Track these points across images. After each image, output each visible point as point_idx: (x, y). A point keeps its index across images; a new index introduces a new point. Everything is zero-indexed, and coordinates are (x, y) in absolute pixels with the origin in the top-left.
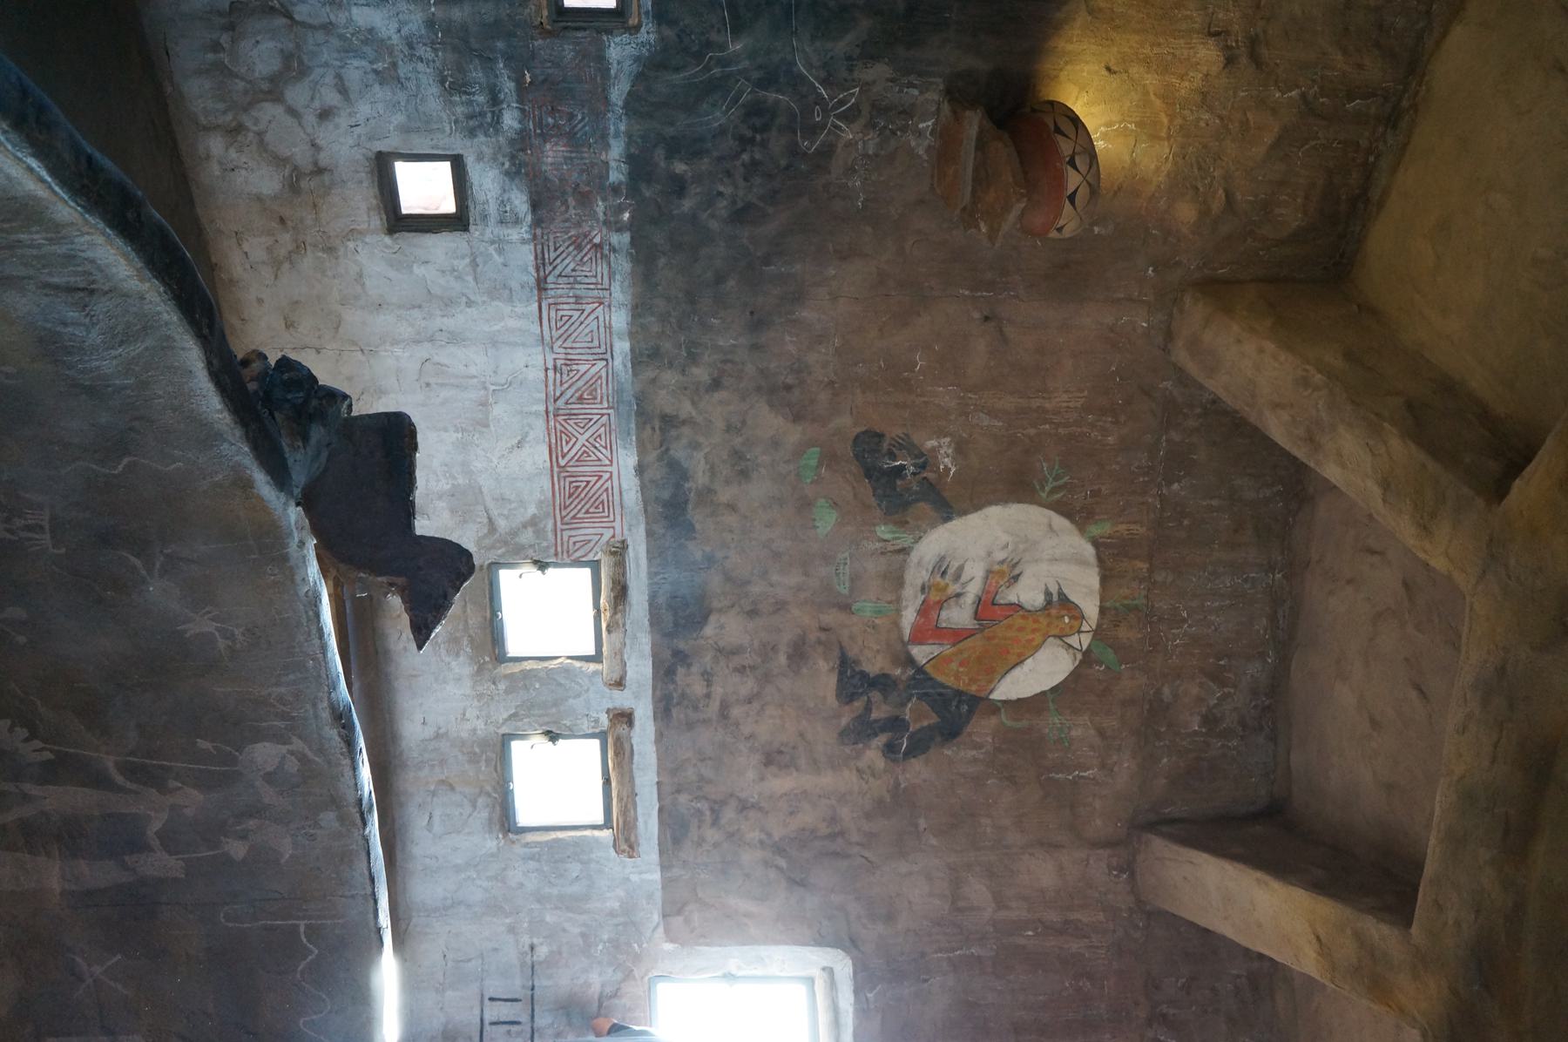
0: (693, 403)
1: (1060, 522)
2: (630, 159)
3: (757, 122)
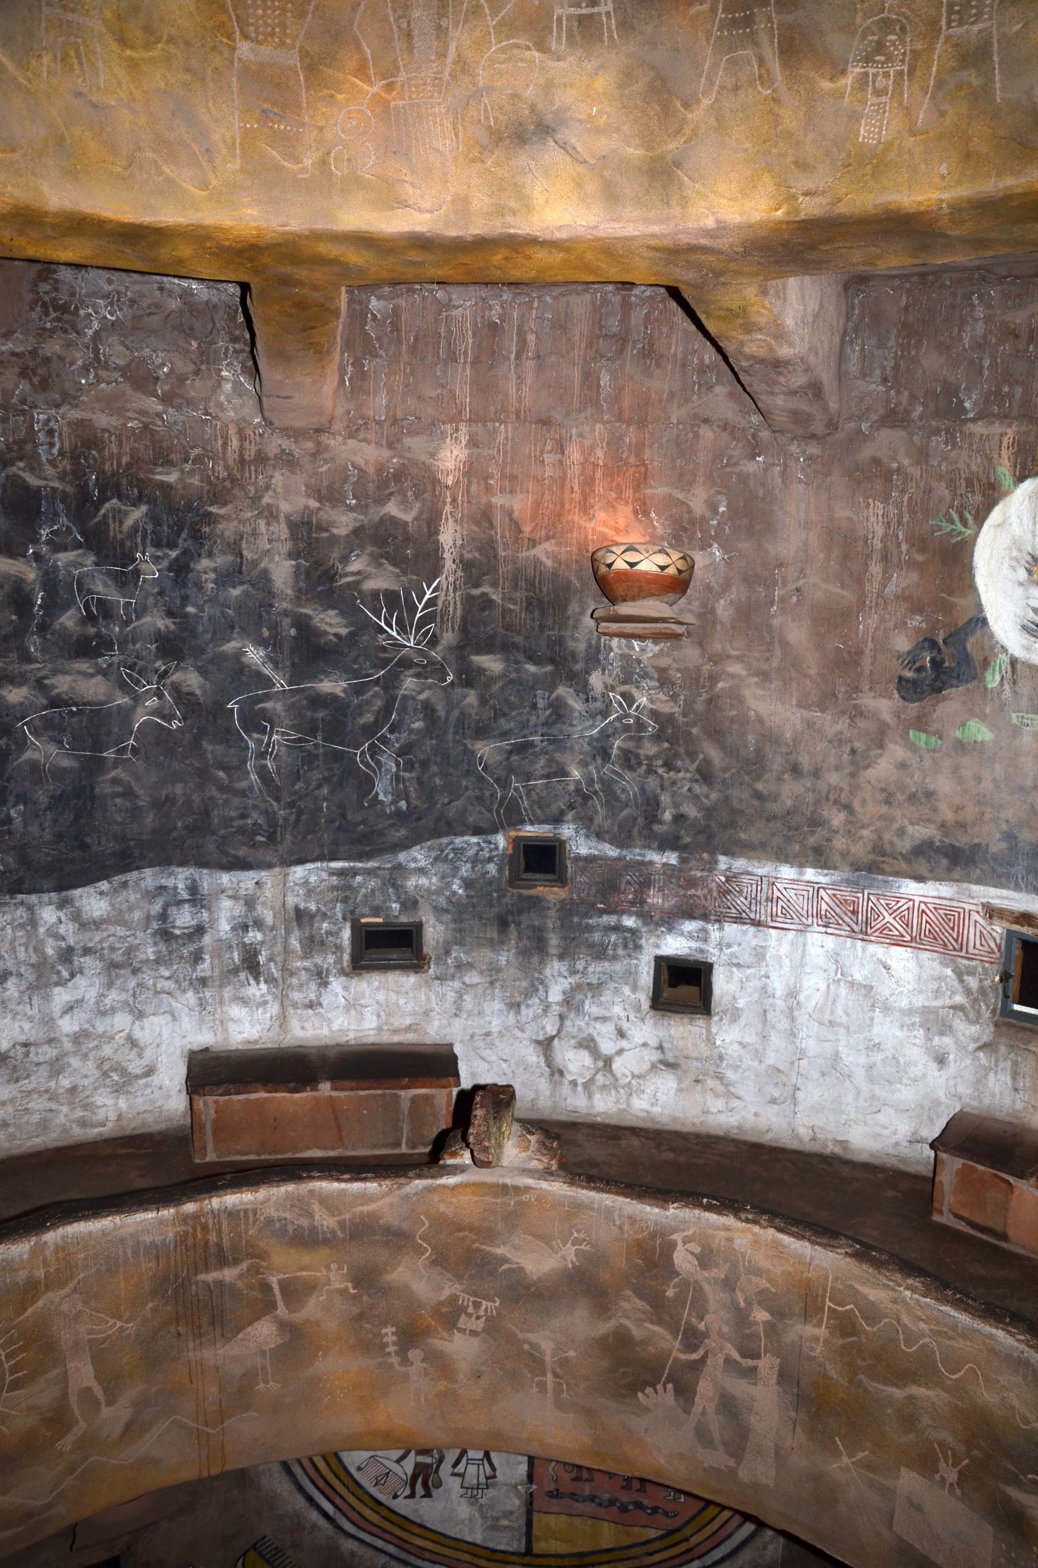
0: (863, 827)
1: (996, 515)
2: (662, 848)
3: (633, 761)
